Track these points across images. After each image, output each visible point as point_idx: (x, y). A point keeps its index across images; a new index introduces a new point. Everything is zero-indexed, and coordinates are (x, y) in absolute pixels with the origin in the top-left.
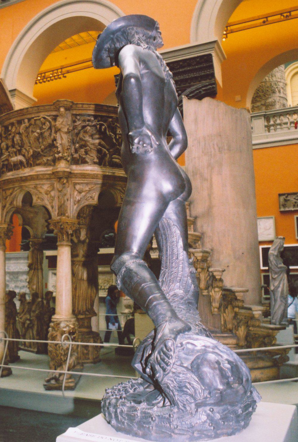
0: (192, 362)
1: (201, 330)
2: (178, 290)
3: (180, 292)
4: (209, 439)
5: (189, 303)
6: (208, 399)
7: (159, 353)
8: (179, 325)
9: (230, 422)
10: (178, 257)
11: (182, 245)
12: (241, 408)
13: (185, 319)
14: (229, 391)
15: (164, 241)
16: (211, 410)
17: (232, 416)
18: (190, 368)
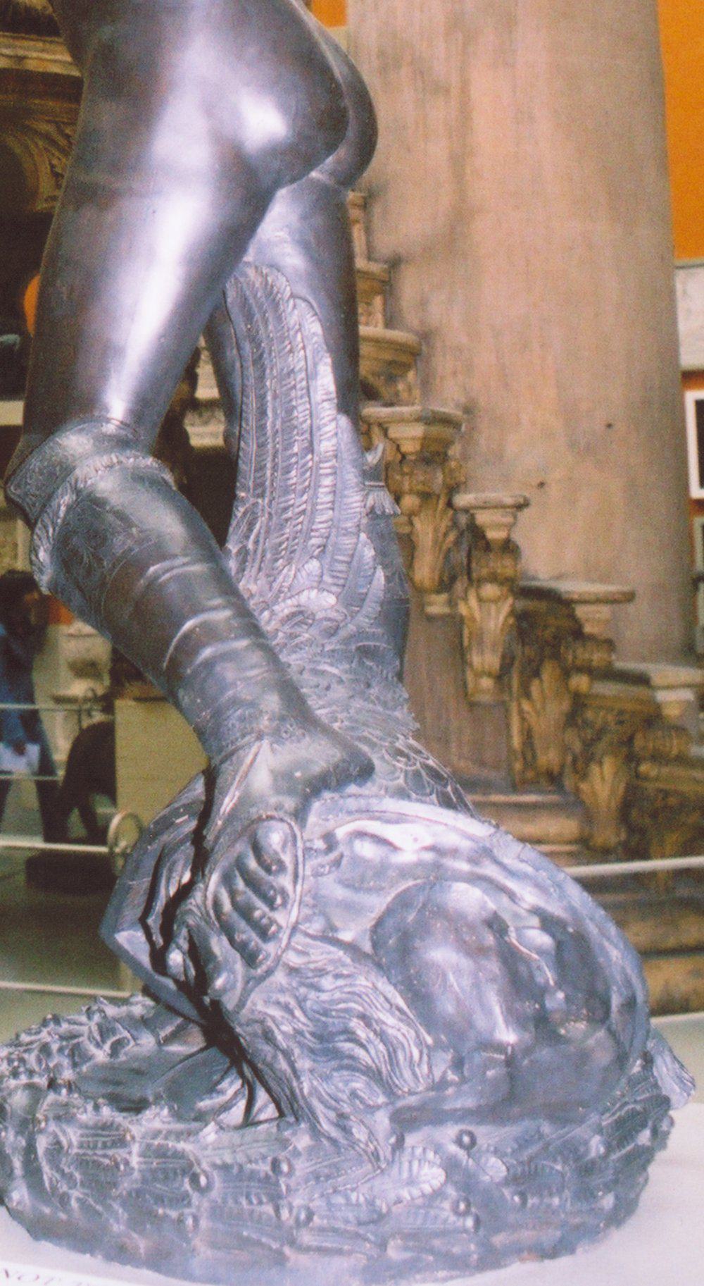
0: (379, 923)
1: (417, 774)
2: (314, 593)
3: (324, 602)
4: (454, 1273)
5: (365, 652)
6: (450, 1091)
7: (227, 880)
8: (317, 754)
9: (551, 1195)
10: (311, 443)
12: (600, 1130)
13: (347, 723)
14: (545, 1054)
16: (466, 1139)
17: (559, 1167)
18: (367, 947)
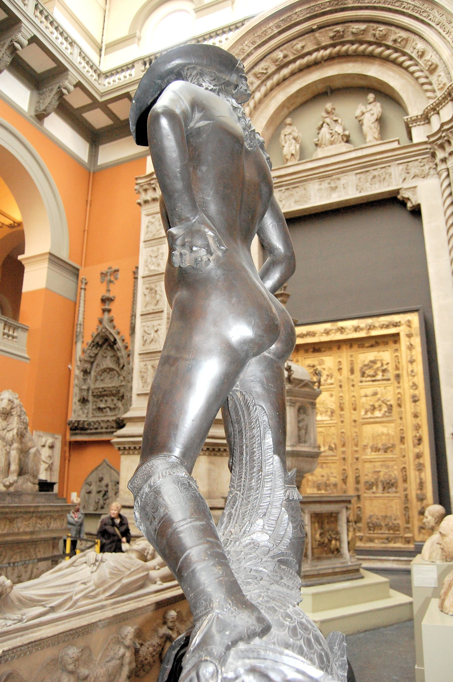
2: (259, 534)
3: (263, 538)
10: (261, 467)
11: (272, 443)
15: (237, 436)
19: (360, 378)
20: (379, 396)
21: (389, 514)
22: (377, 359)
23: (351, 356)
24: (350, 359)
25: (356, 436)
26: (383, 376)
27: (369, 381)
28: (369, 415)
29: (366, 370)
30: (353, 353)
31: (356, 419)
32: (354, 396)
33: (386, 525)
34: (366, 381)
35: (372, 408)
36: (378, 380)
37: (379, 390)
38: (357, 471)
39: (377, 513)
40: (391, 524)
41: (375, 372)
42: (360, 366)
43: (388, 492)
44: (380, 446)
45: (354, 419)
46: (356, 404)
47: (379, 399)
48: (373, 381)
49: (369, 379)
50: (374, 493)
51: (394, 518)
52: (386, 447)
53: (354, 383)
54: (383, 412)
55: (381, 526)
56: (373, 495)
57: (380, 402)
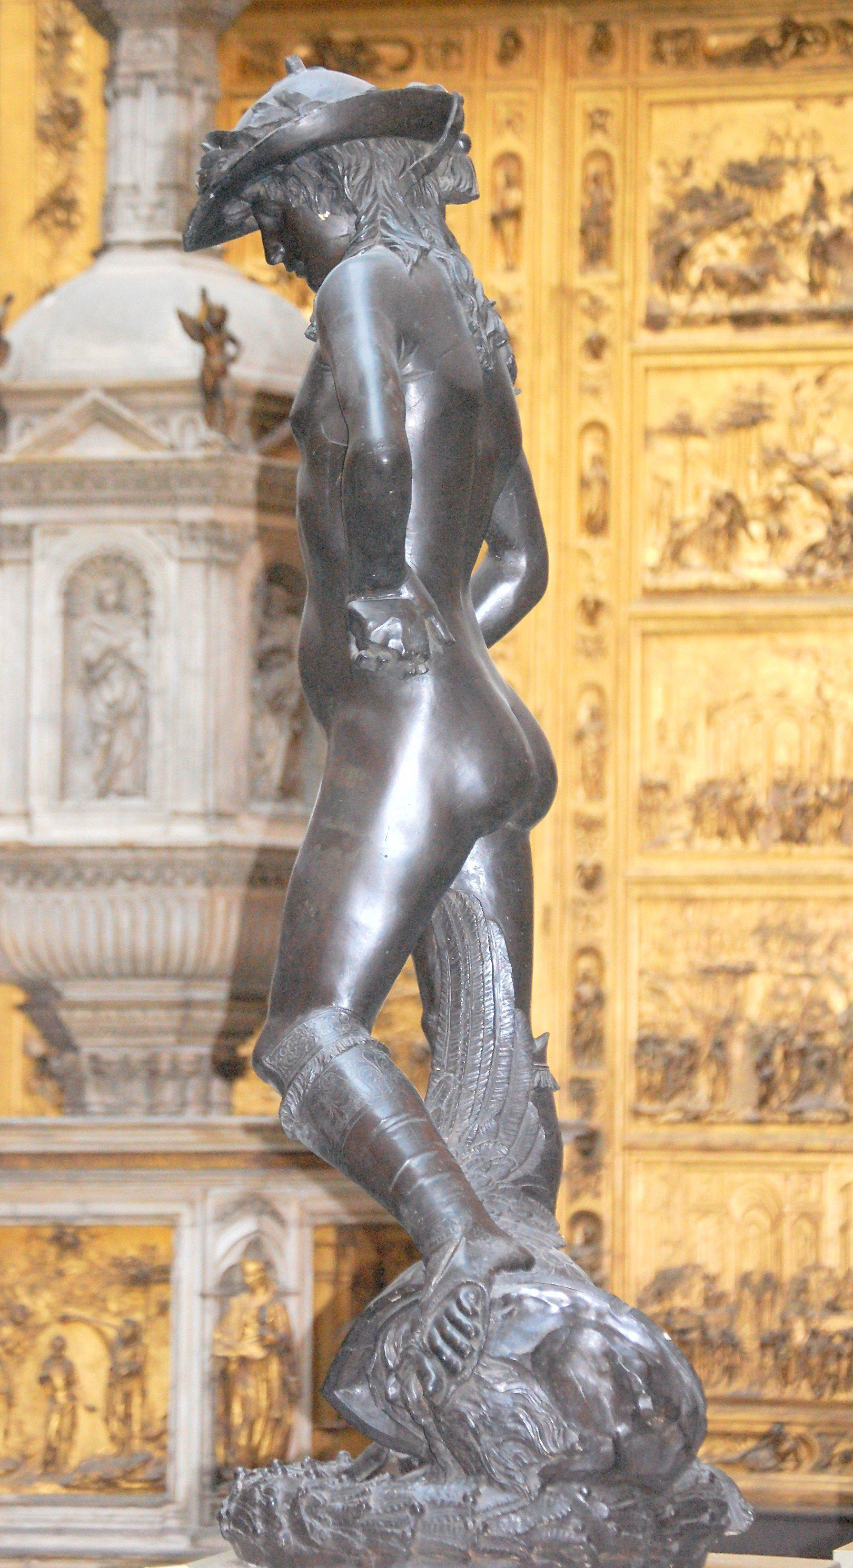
6: (577, 1457)
9: (638, 1532)
17: (644, 1517)
19: (646, 293)
20: (773, 433)
21: (789, 1271)
22: (789, 152)
23: (597, 120)
24: (583, 143)
25: (596, 715)
26: (814, 287)
27: (714, 320)
28: (697, 570)
29: (698, 232)
30: (611, 101)
31: (604, 594)
32: (596, 425)
33: (773, 1342)
34: (688, 321)
35: (722, 519)
36: (779, 319)
37: (779, 384)
38: (586, 963)
39: (710, 1262)
40: (800, 1336)
41: (764, 253)
42: (656, 195)
43: (796, 1118)
44: (758, 792)
45: (590, 591)
46: (605, 483)
47: (773, 458)
48: (741, 320)
49: (713, 302)
50: (696, 1118)
51: (820, 1292)
52: (809, 798)
53: (604, 327)
54: (792, 551)
55: (730, 1343)
56: (691, 1134)
57: (781, 475)
